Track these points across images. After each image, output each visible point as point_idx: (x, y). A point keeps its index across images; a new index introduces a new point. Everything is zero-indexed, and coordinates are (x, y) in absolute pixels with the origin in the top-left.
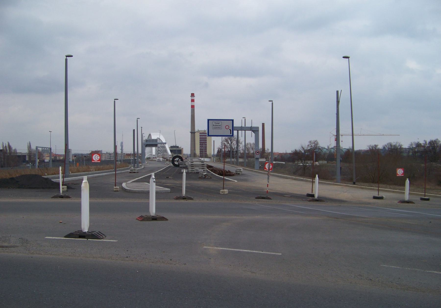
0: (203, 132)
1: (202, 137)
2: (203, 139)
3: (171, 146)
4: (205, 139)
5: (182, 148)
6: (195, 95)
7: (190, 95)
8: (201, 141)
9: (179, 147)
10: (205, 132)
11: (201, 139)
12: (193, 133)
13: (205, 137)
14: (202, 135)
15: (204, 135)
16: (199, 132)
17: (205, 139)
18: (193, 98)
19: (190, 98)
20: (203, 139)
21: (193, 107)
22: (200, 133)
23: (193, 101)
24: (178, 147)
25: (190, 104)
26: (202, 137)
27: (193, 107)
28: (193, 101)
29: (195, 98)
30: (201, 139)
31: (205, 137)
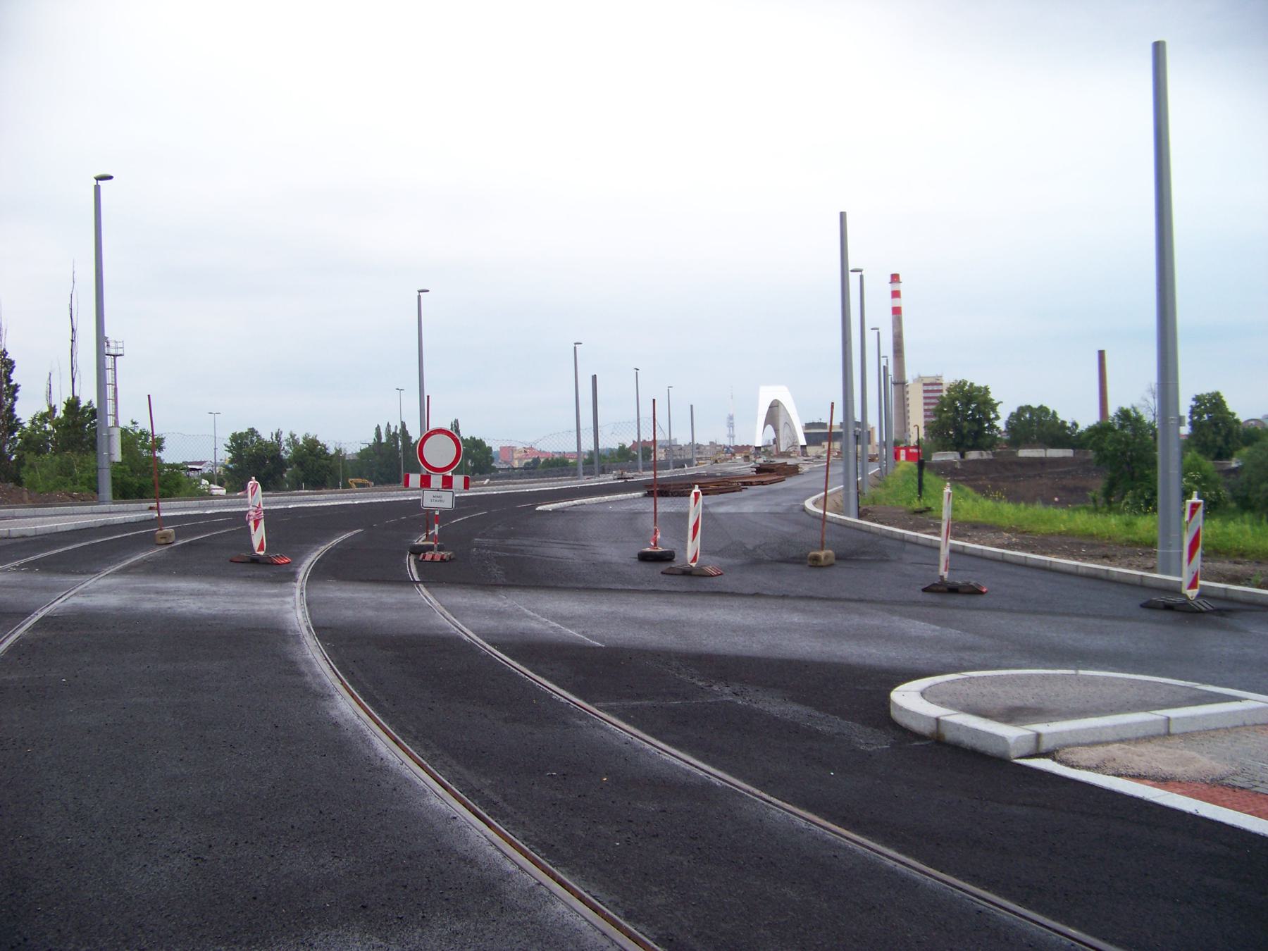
0: (933, 381)
6: (901, 279)
10: (938, 382)
14: (930, 388)
15: (935, 388)
19: (889, 288)
21: (897, 311)
22: (925, 385)
23: (896, 294)
27: (897, 311)
28: (896, 294)
29: (902, 287)
30: (928, 401)
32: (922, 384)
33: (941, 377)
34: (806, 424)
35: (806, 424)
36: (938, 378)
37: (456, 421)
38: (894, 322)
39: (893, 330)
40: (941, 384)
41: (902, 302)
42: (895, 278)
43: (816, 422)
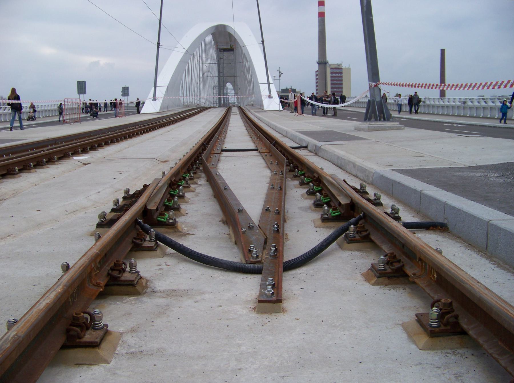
0: (337, 66)
1: (334, 75)
2: (336, 79)
3: (283, 89)
4: (340, 78)
8: (333, 82)
9: (297, 90)
10: (339, 67)
11: (333, 79)
12: (323, 63)
13: (340, 75)
14: (335, 71)
15: (338, 71)
16: (330, 66)
17: (340, 78)
20: (336, 79)
21: (322, 15)
22: (331, 69)
26: (334, 75)
27: (322, 15)
31: (340, 75)
32: (330, 68)
33: (341, 64)
37: (14, 91)
40: (342, 69)
41: (327, 9)
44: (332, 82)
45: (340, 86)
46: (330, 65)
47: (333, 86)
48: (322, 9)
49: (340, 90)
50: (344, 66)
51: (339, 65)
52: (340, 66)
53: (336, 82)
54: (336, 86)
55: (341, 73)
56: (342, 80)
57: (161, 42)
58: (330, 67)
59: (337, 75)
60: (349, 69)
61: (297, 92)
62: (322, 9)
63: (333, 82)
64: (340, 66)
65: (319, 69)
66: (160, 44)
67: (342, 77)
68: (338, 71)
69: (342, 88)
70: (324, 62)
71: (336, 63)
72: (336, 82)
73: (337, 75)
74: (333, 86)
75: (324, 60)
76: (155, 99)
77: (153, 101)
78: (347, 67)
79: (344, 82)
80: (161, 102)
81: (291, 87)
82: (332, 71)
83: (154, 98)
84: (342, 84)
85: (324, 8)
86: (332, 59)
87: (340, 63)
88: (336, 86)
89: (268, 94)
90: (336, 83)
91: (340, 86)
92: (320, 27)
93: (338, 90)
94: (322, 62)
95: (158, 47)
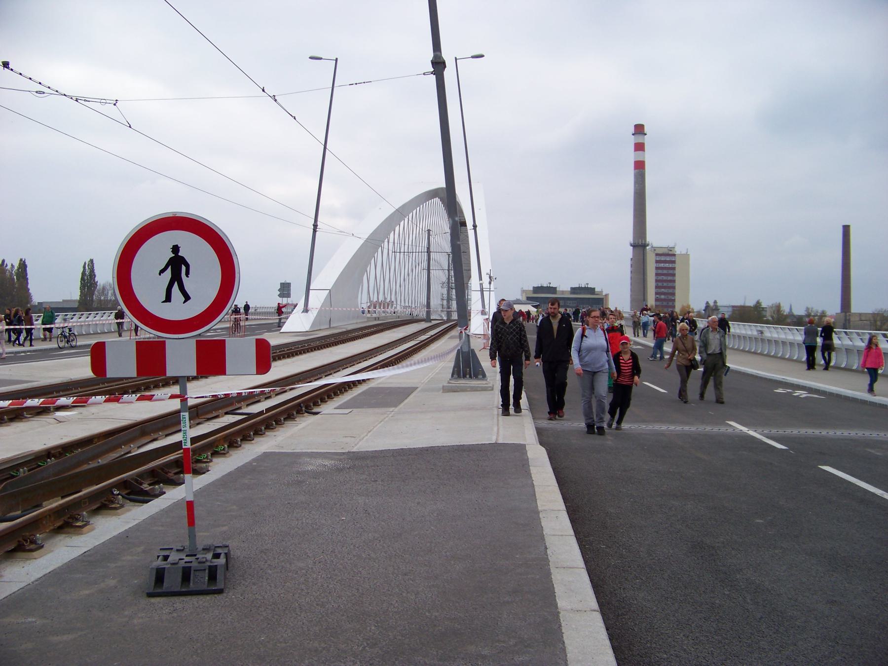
0: (666, 251)
1: (662, 265)
2: (665, 272)
3: (573, 287)
4: (671, 272)
5: (607, 295)
6: (646, 130)
7: (632, 130)
8: (660, 278)
9: (596, 290)
10: (670, 253)
11: (660, 271)
12: (640, 245)
14: (663, 258)
15: (668, 259)
16: (655, 250)
17: (671, 272)
18: (640, 139)
19: (632, 140)
20: (665, 272)
21: (640, 166)
22: (657, 255)
23: (639, 147)
24: (592, 291)
25: (631, 156)
26: (662, 265)
27: (640, 166)
28: (639, 147)
29: (647, 140)
30: (660, 271)
31: (671, 266)
32: (654, 255)
34: (534, 287)
35: (534, 287)
36: (671, 249)
38: (636, 176)
39: (635, 186)
40: (674, 255)
41: (648, 157)
42: (639, 129)
43: (545, 285)
44: (658, 278)
45: (670, 284)
46: (655, 249)
47: (660, 284)
48: (639, 156)
49: (670, 291)
50: (678, 251)
51: (671, 249)
52: (671, 251)
53: (665, 278)
54: (665, 284)
55: (674, 262)
56: (674, 275)
57: (318, 223)
58: (656, 252)
59: (667, 265)
60: (686, 256)
61: (596, 293)
62: (639, 156)
63: (660, 278)
64: (671, 251)
65: (633, 256)
66: (317, 226)
67: (674, 269)
68: (668, 259)
69: (674, 288)
70: (642, 243)
71: (665, 245)
72: (665, 278)
73: (667, 265)
74: (660, 284)
75: (642, 241)
76: (306, 310)
77: (303, 313)
78: (684, 252)
79: (677, 278)
80: (315, 316)
81: (587, 284)
82: (658, 259)
83: (305, 308)
84: (674, 281)
85: (644, 154)
86: (656, 238)
87: (671, 245)
88: (665, 284)
89: (481, 308)
90: (664, 279)
91: (670, 284)
92: (637, 185)
93: (668, 291)
94: (639, 243)
95: (315, 231)
